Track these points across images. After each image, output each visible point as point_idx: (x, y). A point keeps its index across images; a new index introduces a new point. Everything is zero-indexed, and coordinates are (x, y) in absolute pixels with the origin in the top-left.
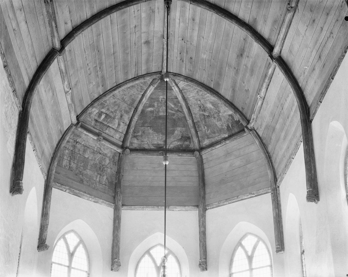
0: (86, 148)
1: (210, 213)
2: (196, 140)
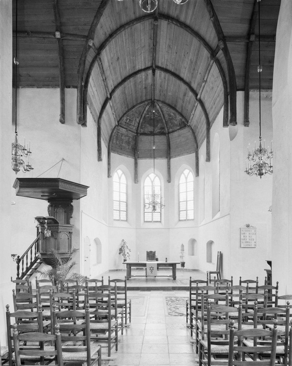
0: (122, 134)
1: (172, 160)
2: (166, 129)
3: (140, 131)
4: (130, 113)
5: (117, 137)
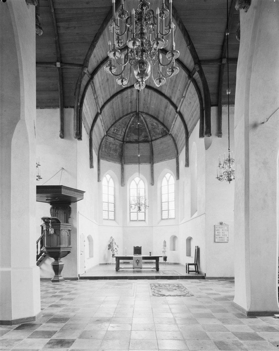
0: (110, 143)
1: (155, 165)
2: (150, 137)
3: (126, 139)
4: (118, 124)
5: (106, 146)
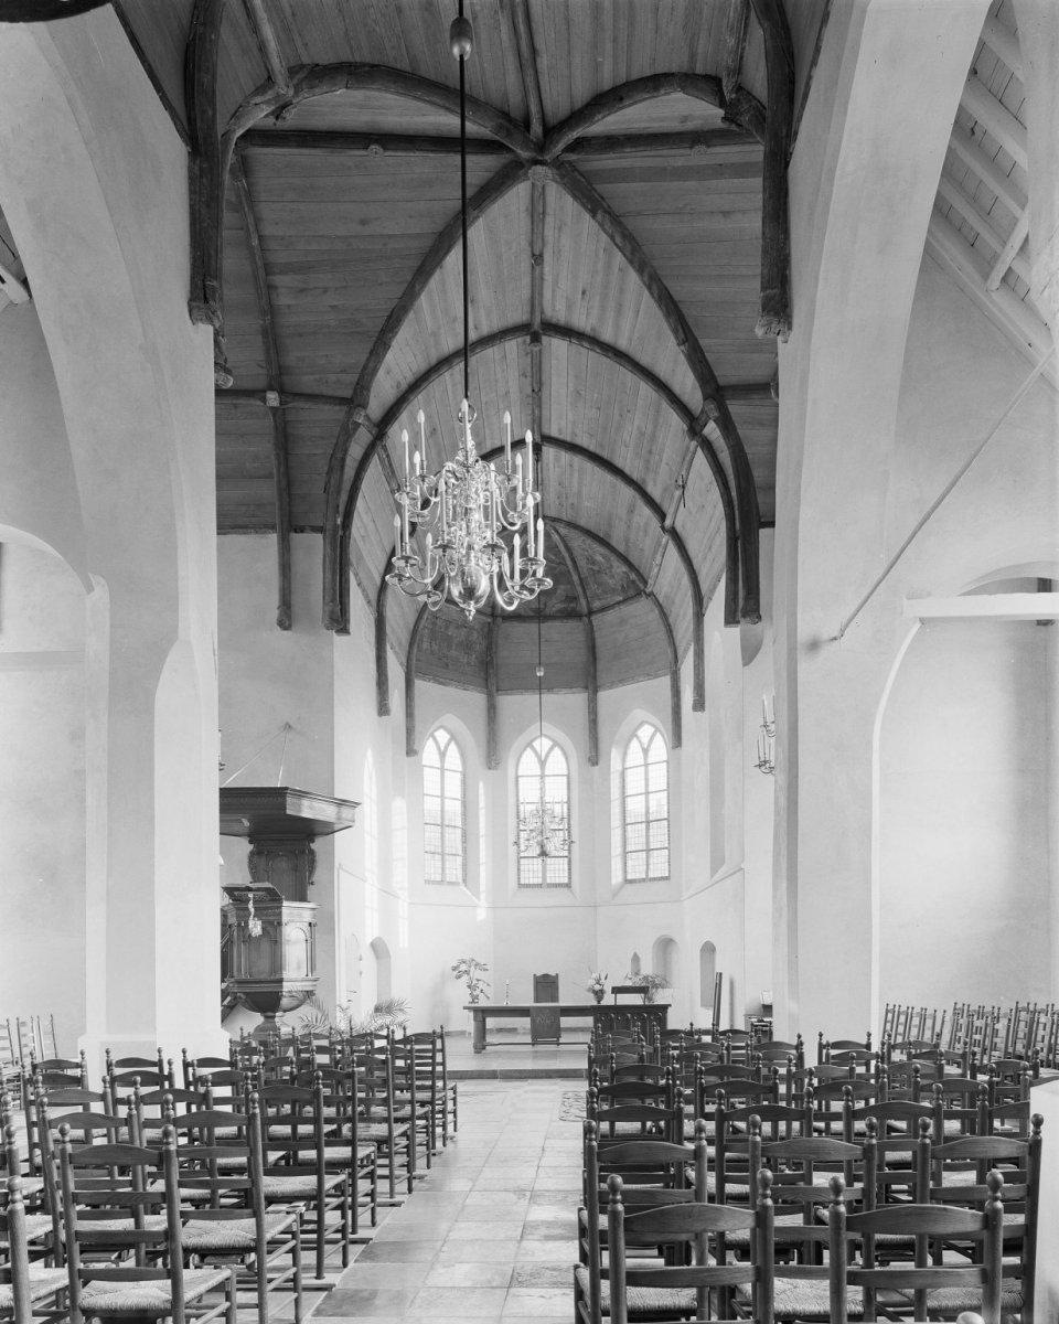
1: (602, 695)
2: (583, 601)
5: (433, 632)
